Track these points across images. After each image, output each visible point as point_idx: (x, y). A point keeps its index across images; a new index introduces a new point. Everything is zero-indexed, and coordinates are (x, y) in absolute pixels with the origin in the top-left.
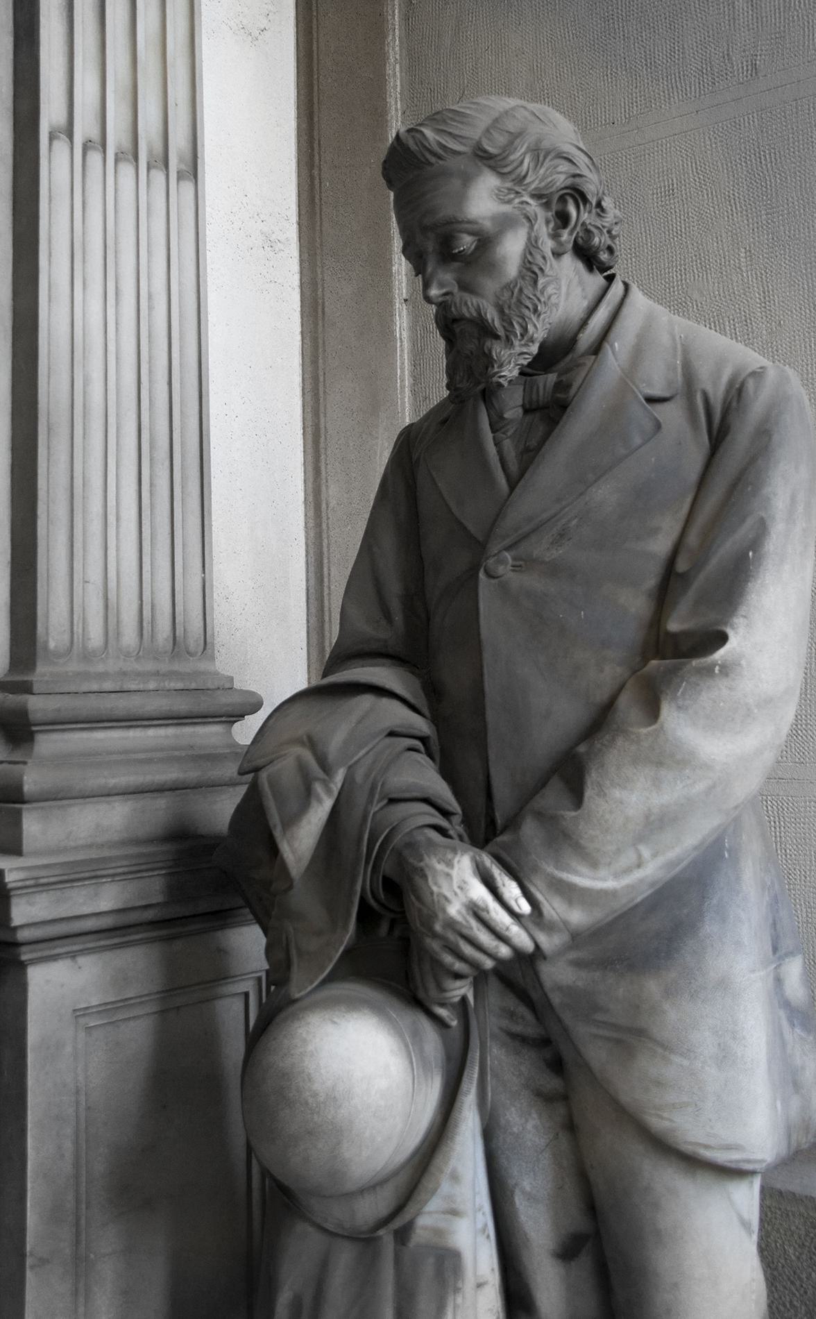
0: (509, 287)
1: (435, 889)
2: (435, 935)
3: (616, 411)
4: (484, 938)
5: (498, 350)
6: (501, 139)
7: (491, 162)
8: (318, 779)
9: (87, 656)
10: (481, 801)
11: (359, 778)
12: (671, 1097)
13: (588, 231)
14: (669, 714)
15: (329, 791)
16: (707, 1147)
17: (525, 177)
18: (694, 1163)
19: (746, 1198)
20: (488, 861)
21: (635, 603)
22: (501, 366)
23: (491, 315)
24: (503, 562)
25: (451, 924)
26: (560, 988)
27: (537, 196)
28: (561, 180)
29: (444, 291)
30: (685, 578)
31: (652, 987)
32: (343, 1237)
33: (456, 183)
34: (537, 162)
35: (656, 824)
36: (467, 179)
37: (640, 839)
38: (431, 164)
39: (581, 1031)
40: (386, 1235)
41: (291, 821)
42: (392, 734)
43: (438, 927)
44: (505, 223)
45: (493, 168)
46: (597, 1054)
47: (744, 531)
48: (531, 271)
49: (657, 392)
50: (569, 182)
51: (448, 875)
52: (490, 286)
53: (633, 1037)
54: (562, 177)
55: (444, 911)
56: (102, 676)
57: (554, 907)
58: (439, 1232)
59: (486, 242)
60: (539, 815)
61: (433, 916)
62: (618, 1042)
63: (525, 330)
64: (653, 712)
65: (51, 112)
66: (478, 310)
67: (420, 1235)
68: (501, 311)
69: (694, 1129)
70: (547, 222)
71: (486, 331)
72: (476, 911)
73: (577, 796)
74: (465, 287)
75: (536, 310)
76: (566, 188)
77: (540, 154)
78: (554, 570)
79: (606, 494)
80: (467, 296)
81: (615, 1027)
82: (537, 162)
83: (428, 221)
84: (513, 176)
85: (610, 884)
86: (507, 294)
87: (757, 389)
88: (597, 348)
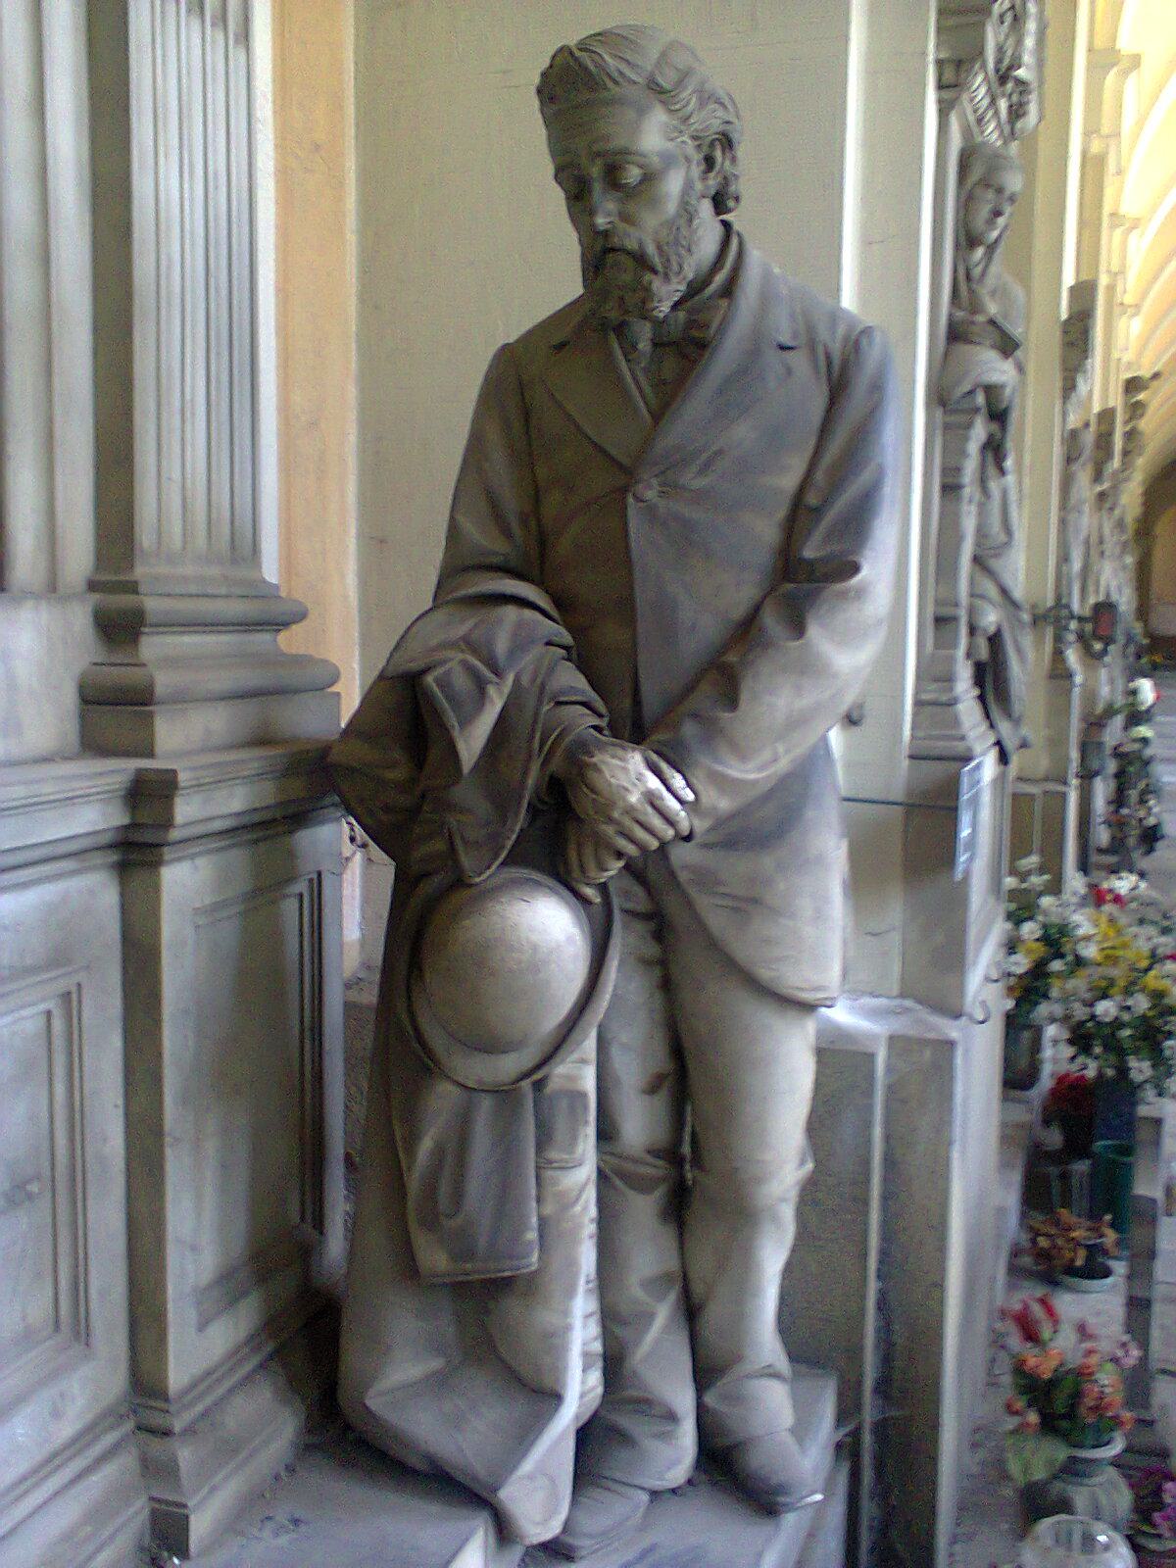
0: (670, 224)
1: (613, 781)
2: (610, 820)
3: (754, 352)
4: (657, 822)
5: (657, 284)
7: (663, 97)
8: (491, 682)
10: (627, 703)
11: (525, 680)
13: (725, 178)
14: (814, 631)
15: (500, 692)
16: (802, 989)
17: (688, 118)
20: (655, 757)
21: (765, 530)
22: (660, 301)
23: (651, 249)
24: (650, 487)
25: (630, 811)
26: (685, 867)
27: (694, 138)
28: (716, 125)
29: (608, 220)
30: (817, 512)
31: (767, 862)
32: (483, 1091)
33: (631, 114)
36: (642, 112)
38: (606, 88)
39: (703, 902)
40: (526, 1084)
41: (466, 722)
42: (549, 643)
43: (616, 815)
44: (669, 160)
45: (662, 102)
46: (717, 921)
47: (865, 477)
48: (688, 213)
49: (785, 339)
50: (721, 128)
51: (625, 769)
53: (750, 904)
54: (719, 121)
55: (624, 799)
59: (649, 178)
60: (695, 716)
61: (611, 804)
62: (736, 910)
63: (681, 267)
64: (798, 628)
66: (641, 244)
67: (552, 1086)
68: (659, 248)
69: (795, 978)
70: (698, 164)
71: (641, 260)
72: (651, 799)
73: (732, 701)
74: (625, 218)
75: (689, 250)
76: (717, 133)
77: (706, 98)
78: (699, 497)
79: (743, 433)
80: (631, 230)
81: (734, 897)
83: (599, 147)
84: (680, 114)
85: (752, 776)
86: (665, 232)
87: (870, 344)
88: (729, 290)
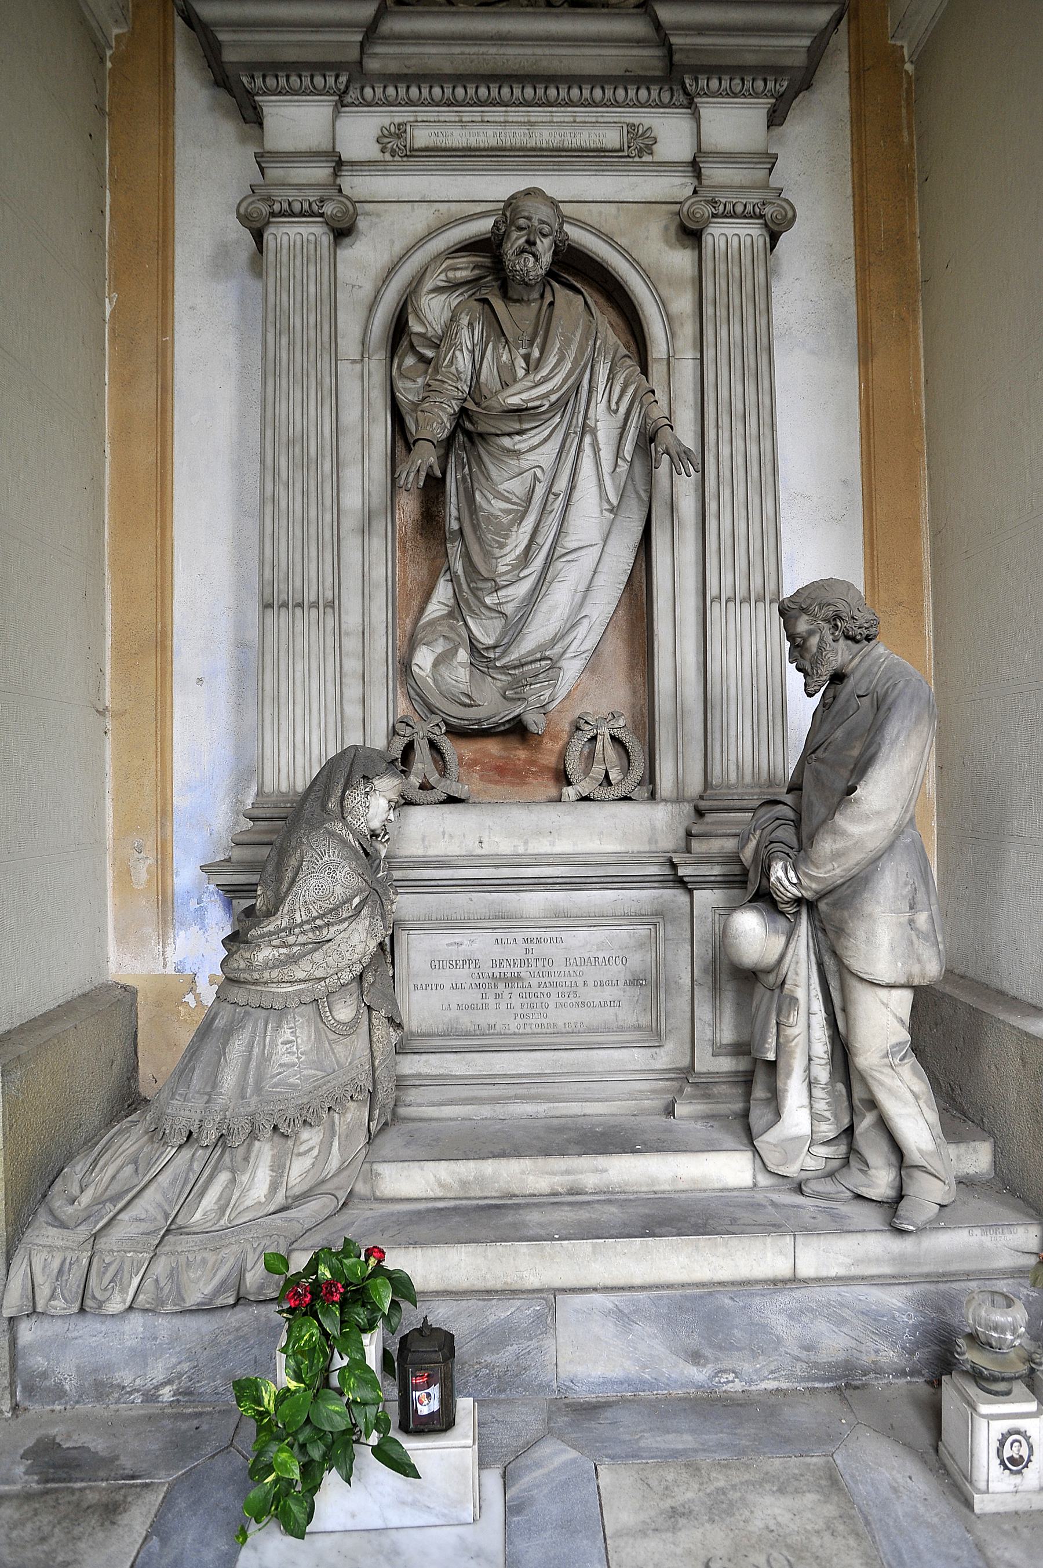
0: (813, 656)
6: (809, 601)
9: (728, 787)
12: (850, 953)
18: (862, 979)
19: (902, 1001)
31: (846, 914)
34: (821, 609)
35: (836, 856)
36: (797, 618)
37: (832, 860)
44: (811, 633)
49: (861, 693)
52: (808, 656)
56: (733, 794)
57: (805, 882)
58: (791, 991)
59: (805, 640)
65: (712, 591)
67: (786, 991)
69: (856, 964)
72: (778, 879)
81: (836, 927)
82: (821, 609)
